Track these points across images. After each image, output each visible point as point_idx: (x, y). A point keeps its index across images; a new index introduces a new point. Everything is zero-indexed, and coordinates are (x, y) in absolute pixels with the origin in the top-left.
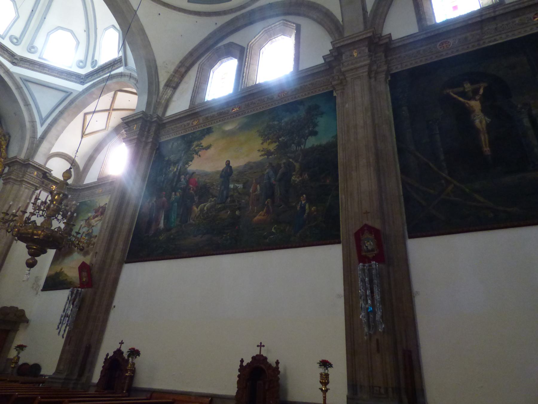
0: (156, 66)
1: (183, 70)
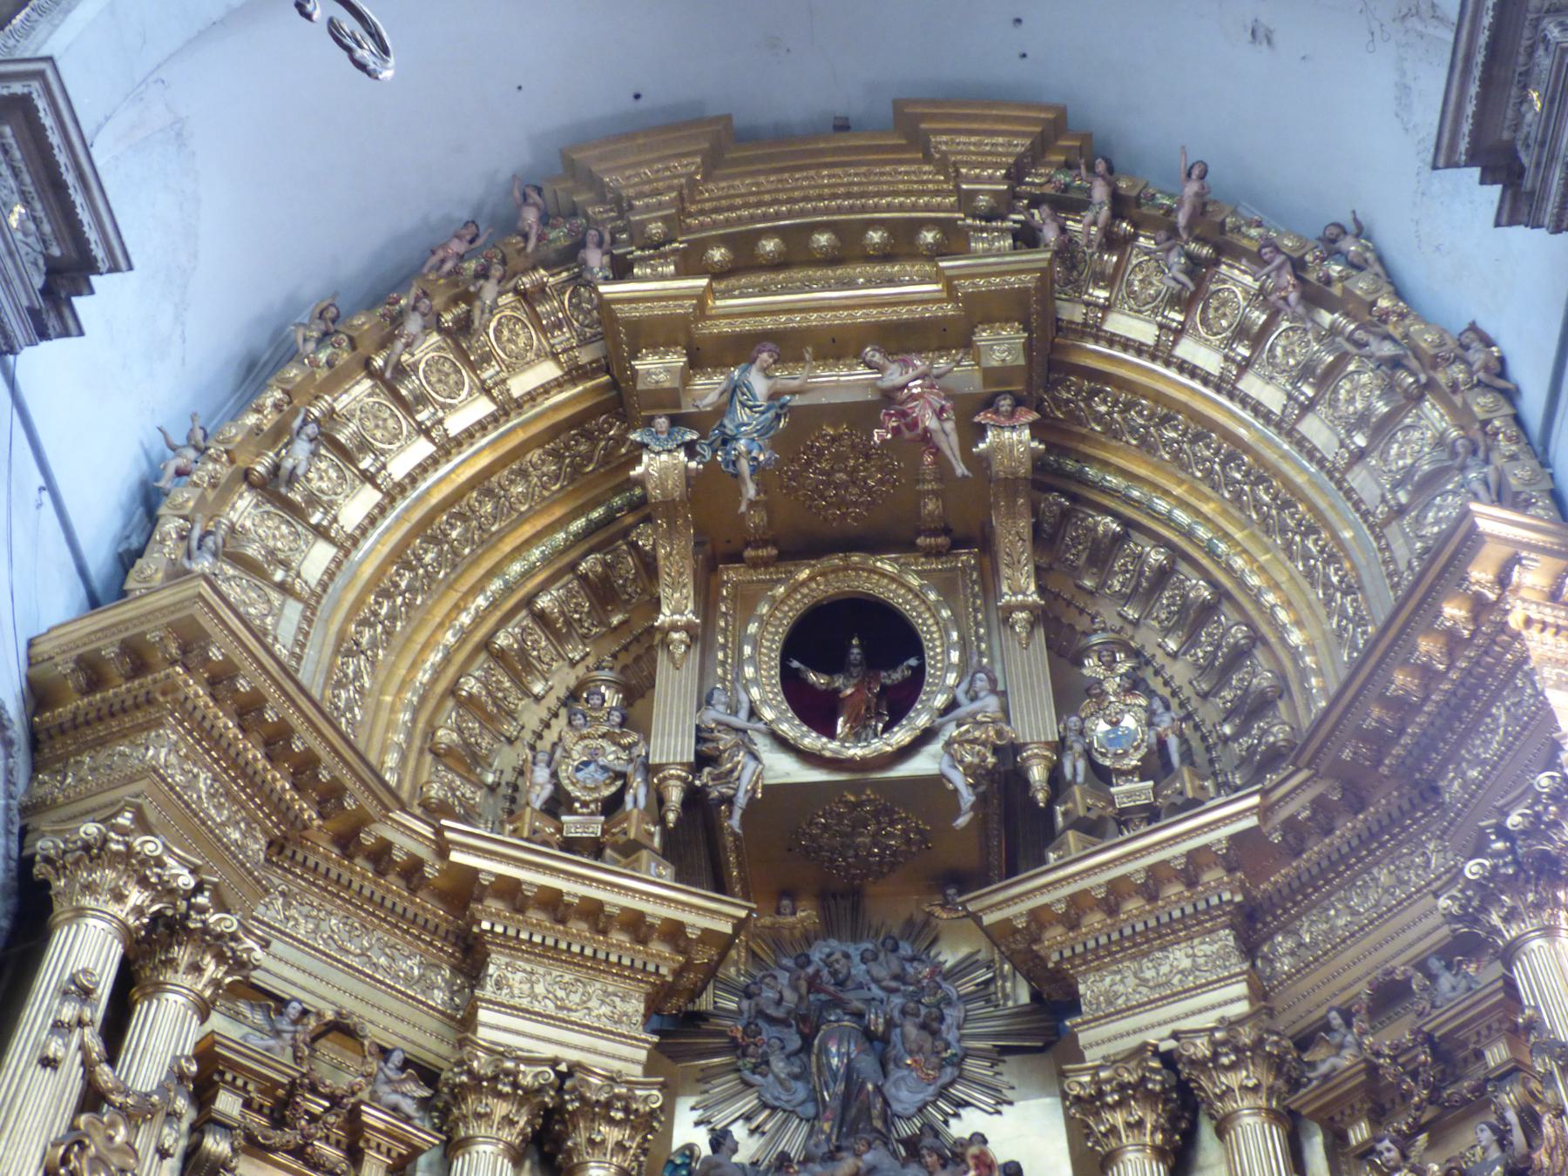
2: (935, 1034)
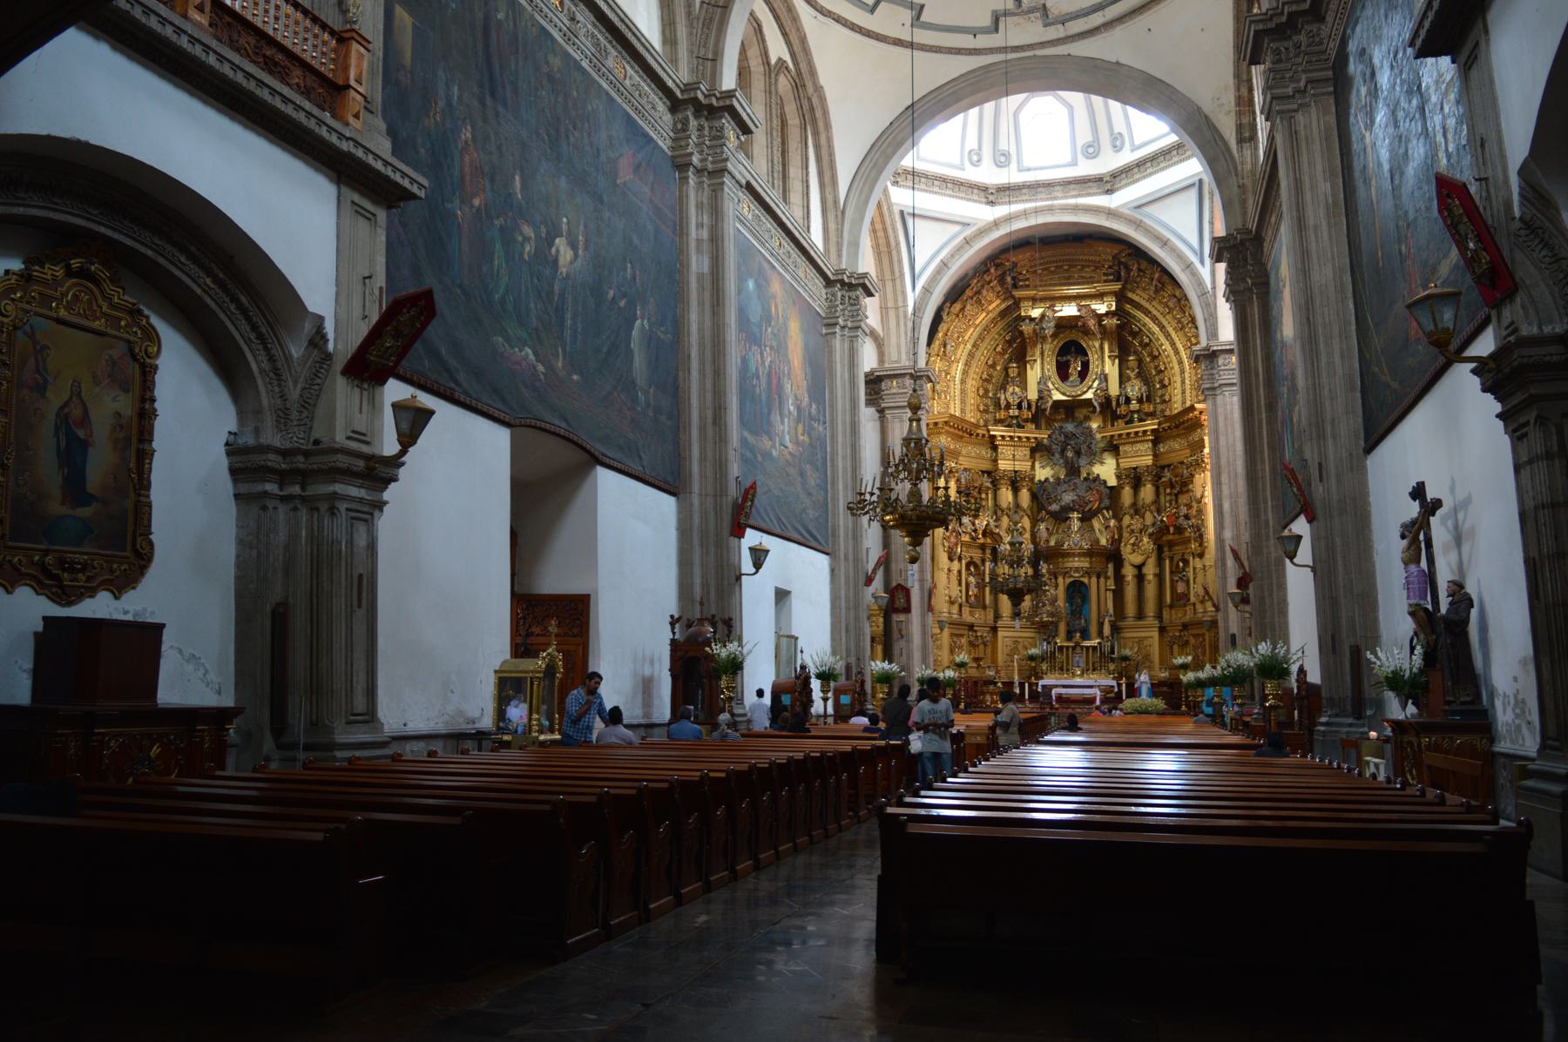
0: (1206, 117)
1: (1244, 91)
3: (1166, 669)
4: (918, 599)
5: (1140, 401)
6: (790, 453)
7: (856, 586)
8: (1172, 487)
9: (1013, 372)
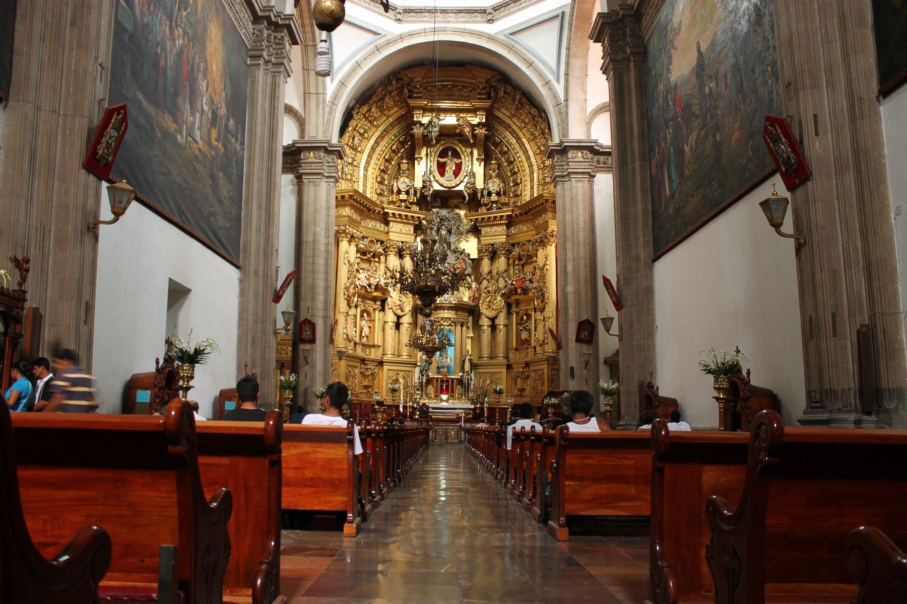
2: (459, 229)
3: (512, 396)
4: (322, 333)
5: (498, 194)
6: (200, 150)
7: (264, 301)
8: (520, 259)
9: (404, 167)
